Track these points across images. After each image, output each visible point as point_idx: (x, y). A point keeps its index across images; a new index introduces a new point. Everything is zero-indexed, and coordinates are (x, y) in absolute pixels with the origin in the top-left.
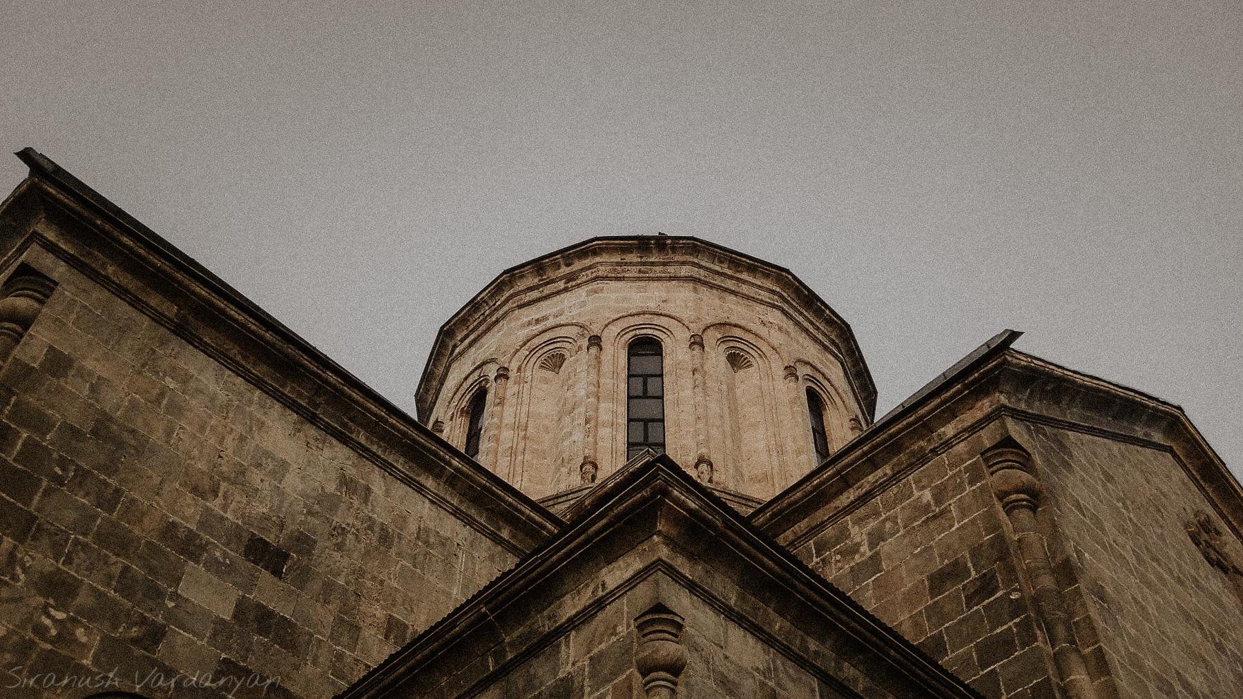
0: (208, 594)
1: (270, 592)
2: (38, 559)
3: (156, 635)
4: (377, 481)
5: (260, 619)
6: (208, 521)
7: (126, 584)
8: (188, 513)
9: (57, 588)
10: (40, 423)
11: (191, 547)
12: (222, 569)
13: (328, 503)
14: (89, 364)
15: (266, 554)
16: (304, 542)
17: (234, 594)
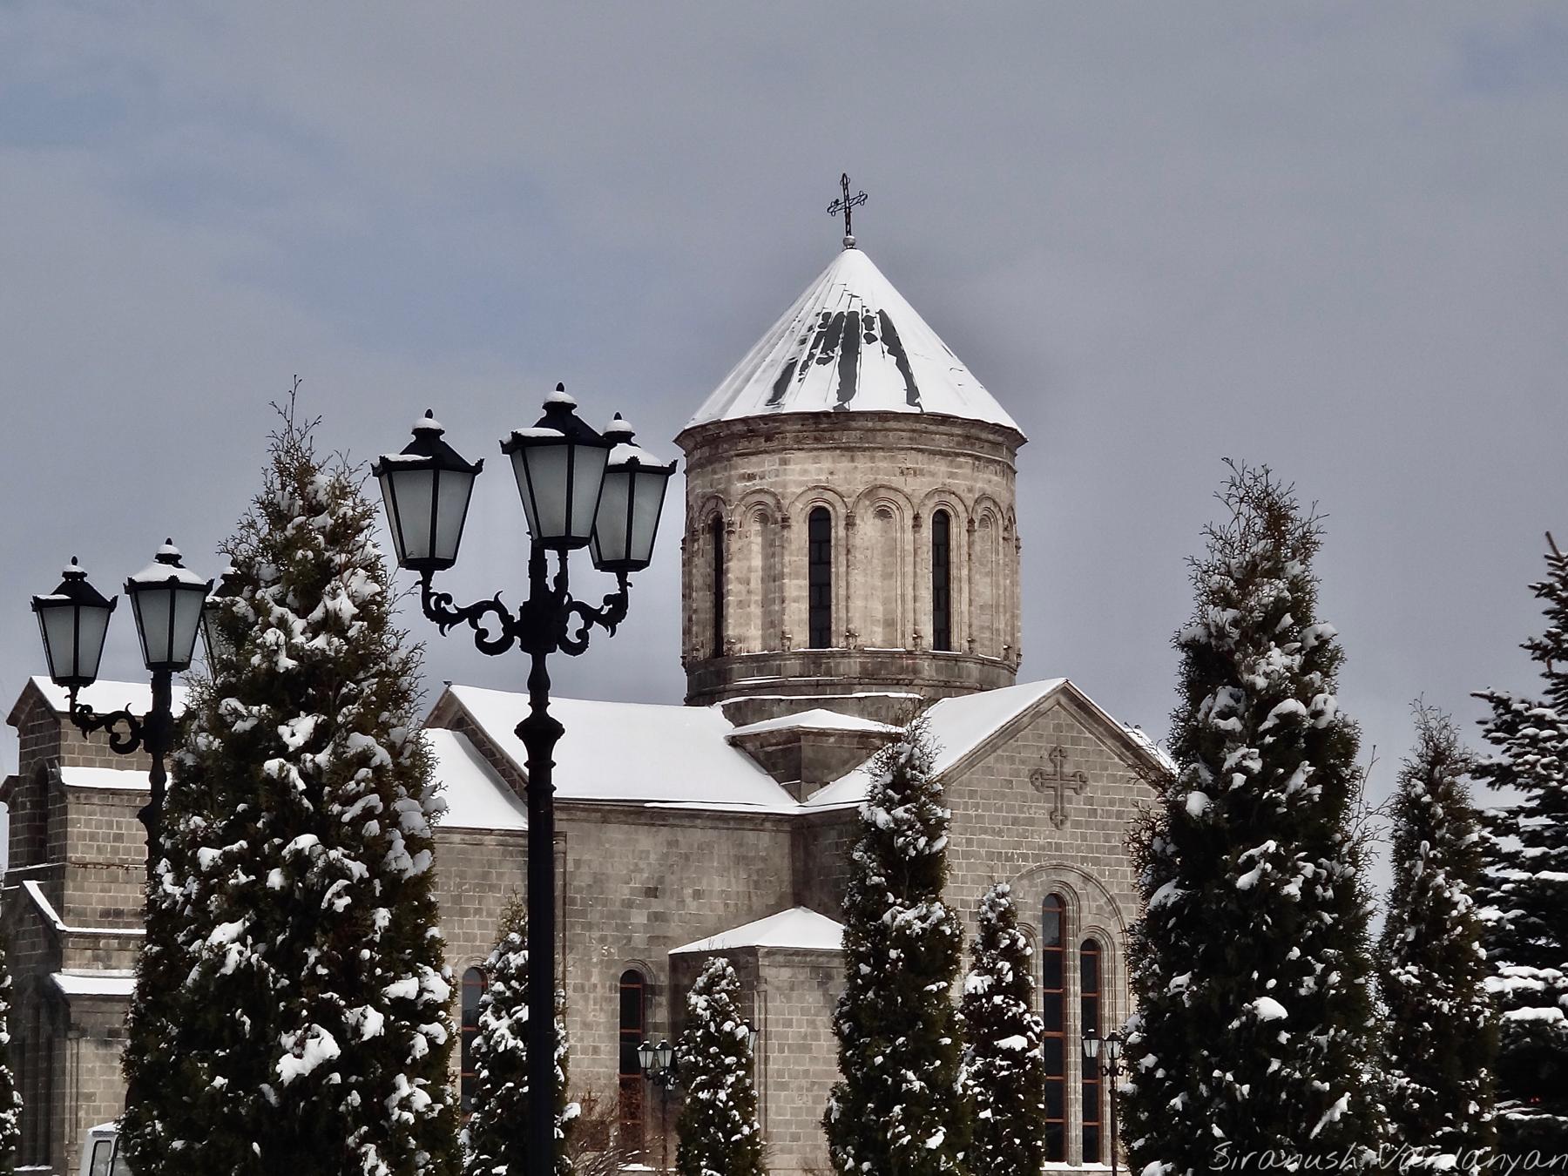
0: (639, 918)
1: (657, 906)
2: (596, 934)
3: (629, 939)
4: (680, 835)
5: (656, 917)
6: (633, 891)
7: (617, 928)
8: (624, 892)
9: (603, 940)
10: (579, 890)
11: (629, 904)
12: (640, 907)
13: (666, 856)
14: (586, 857)
15: (652, 892)
16: (661, 880)
17: (645, 912)
